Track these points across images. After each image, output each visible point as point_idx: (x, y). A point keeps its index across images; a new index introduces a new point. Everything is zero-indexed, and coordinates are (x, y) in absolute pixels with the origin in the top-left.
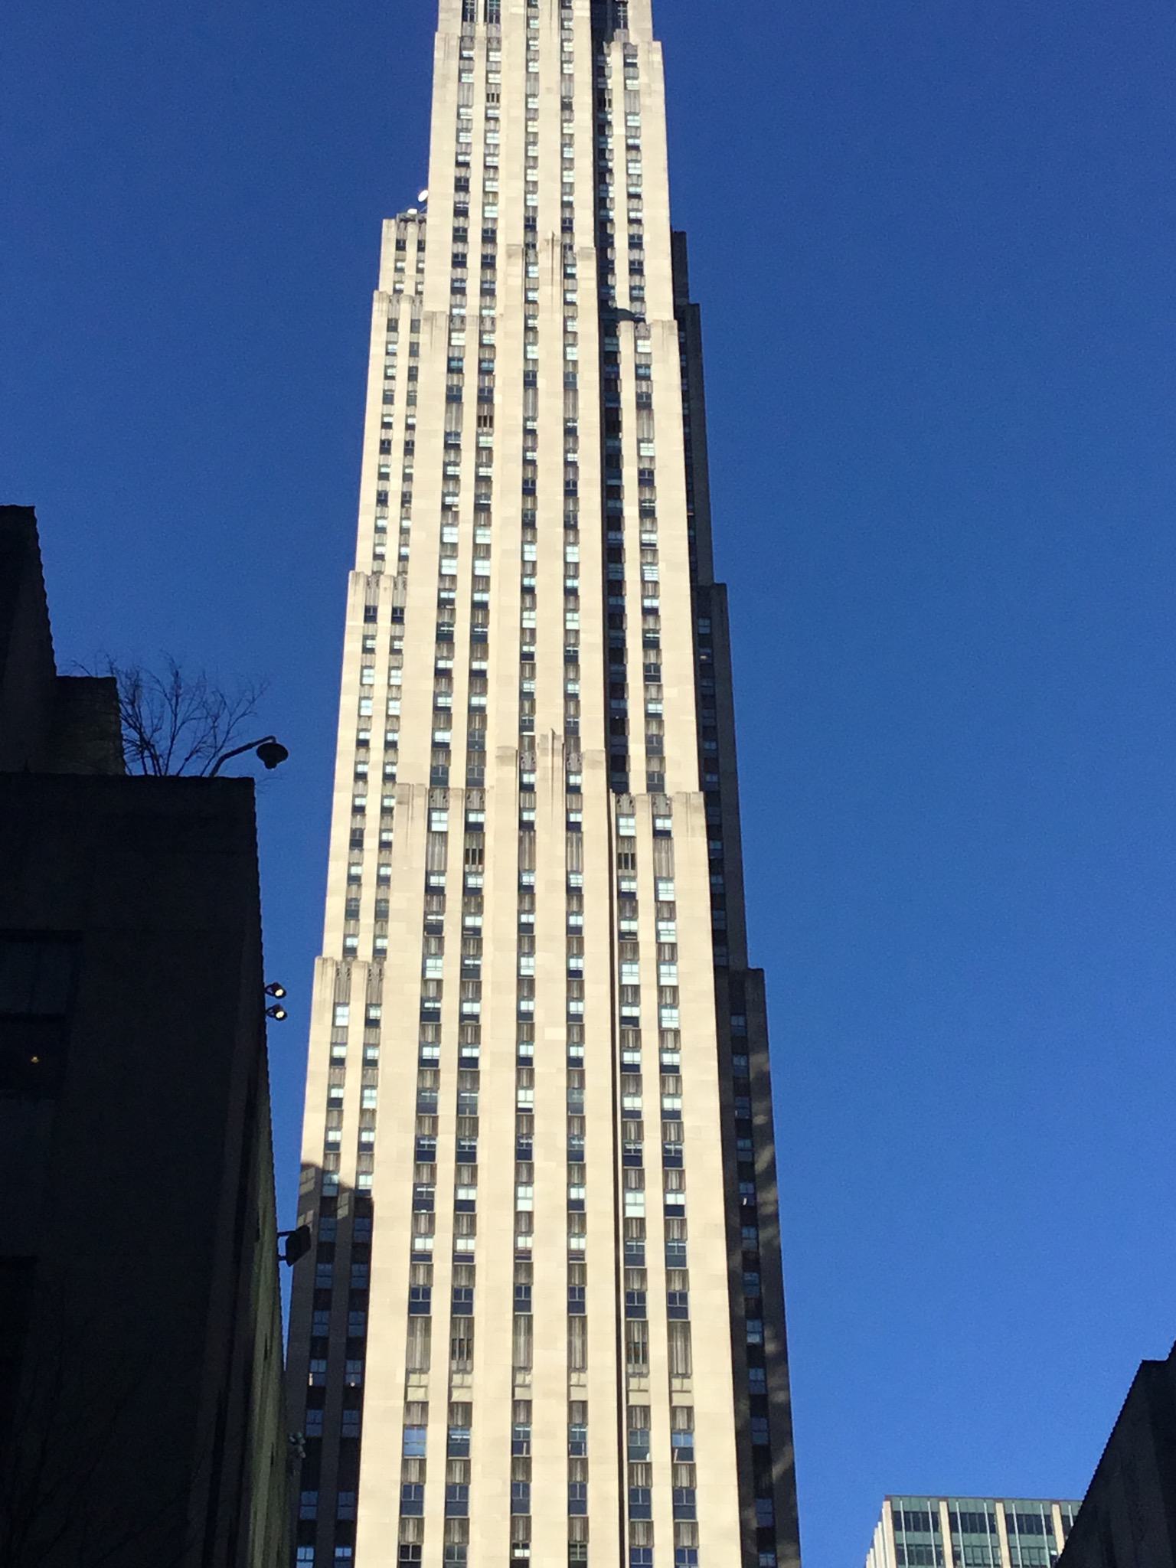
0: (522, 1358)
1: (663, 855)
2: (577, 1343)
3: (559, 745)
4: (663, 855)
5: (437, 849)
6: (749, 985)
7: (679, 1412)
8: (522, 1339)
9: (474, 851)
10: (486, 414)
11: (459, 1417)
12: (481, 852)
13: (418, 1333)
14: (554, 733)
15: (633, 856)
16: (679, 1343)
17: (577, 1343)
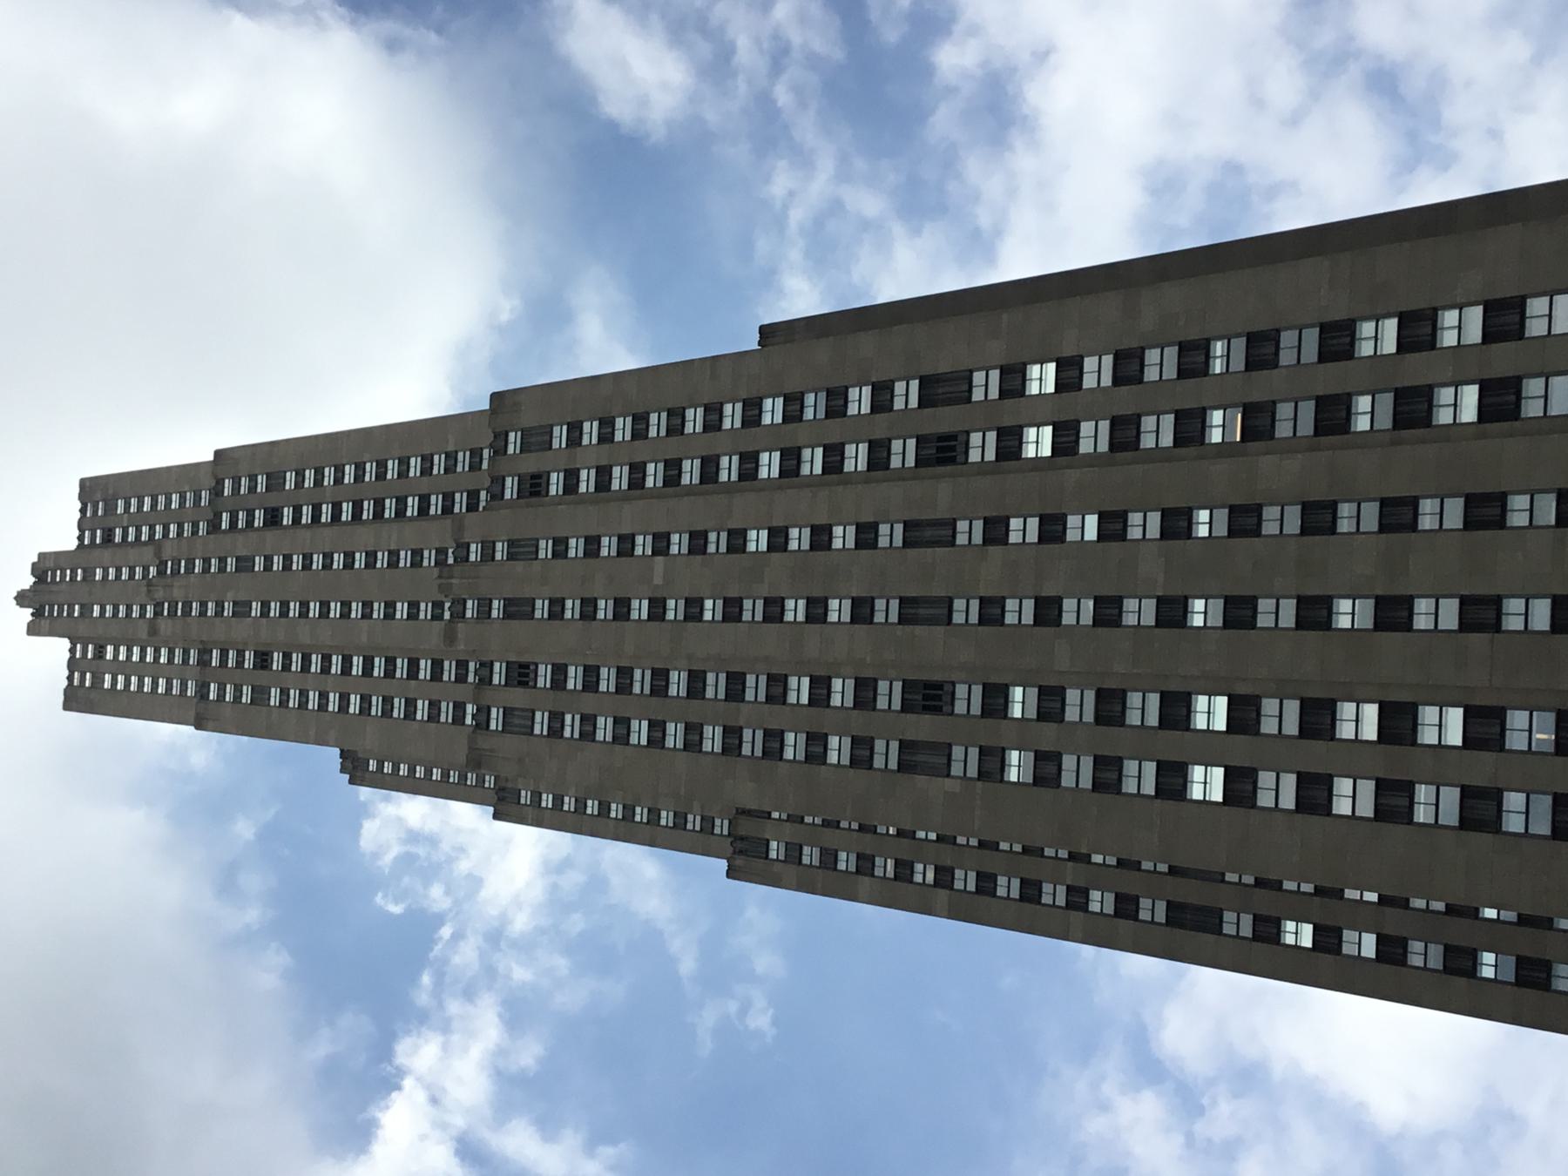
1: (533, 440)
2: (928, 533)
5: (516, 721)
7: (1005, 387)
16: (940, 391)
17: (928, 533)
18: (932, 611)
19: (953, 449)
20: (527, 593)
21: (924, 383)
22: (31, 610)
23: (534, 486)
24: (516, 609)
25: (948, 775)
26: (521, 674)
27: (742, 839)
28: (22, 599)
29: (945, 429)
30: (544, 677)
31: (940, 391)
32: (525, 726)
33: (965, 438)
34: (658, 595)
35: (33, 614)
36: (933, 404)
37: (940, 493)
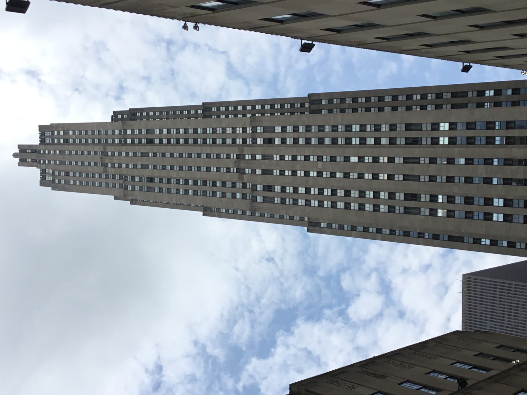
0: (417, 178)
1: (268, 129)
2: (412, 160)
3: (237, 162)
4: (268, 129)
5: (268, 200)
6: (312, 98)
7: (433, 128)
8: (411, 178)
9: (268, 188)
10: (149, 180)
11: (435, 199)
12: (268, 186)
13: (409, 211)
14: (234, 163)
15: (268, 139)
16: (412, 127)
17: (412, 160)
18: (415, 178)
19: (418, 141)
20: (270, 168)
21: (407, 125)
22: (19, 159)
23: (269, 141)
24: (267, 172)
25: (420, 215)
26: (269, 188)
27: (311, 222)
28: (15, 155)
29: (414, 136)
30: (277, 189)
31: (412, 127)
32: (273, 201)
33: (421, 139)
34: (320, 171)
35: (19, 160)
36: (410, 130)
37: (414, 151)
